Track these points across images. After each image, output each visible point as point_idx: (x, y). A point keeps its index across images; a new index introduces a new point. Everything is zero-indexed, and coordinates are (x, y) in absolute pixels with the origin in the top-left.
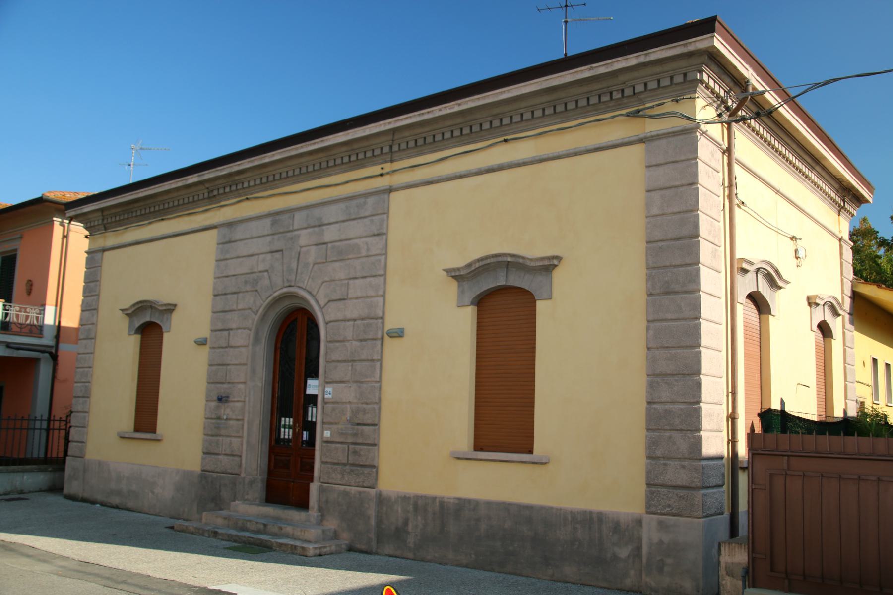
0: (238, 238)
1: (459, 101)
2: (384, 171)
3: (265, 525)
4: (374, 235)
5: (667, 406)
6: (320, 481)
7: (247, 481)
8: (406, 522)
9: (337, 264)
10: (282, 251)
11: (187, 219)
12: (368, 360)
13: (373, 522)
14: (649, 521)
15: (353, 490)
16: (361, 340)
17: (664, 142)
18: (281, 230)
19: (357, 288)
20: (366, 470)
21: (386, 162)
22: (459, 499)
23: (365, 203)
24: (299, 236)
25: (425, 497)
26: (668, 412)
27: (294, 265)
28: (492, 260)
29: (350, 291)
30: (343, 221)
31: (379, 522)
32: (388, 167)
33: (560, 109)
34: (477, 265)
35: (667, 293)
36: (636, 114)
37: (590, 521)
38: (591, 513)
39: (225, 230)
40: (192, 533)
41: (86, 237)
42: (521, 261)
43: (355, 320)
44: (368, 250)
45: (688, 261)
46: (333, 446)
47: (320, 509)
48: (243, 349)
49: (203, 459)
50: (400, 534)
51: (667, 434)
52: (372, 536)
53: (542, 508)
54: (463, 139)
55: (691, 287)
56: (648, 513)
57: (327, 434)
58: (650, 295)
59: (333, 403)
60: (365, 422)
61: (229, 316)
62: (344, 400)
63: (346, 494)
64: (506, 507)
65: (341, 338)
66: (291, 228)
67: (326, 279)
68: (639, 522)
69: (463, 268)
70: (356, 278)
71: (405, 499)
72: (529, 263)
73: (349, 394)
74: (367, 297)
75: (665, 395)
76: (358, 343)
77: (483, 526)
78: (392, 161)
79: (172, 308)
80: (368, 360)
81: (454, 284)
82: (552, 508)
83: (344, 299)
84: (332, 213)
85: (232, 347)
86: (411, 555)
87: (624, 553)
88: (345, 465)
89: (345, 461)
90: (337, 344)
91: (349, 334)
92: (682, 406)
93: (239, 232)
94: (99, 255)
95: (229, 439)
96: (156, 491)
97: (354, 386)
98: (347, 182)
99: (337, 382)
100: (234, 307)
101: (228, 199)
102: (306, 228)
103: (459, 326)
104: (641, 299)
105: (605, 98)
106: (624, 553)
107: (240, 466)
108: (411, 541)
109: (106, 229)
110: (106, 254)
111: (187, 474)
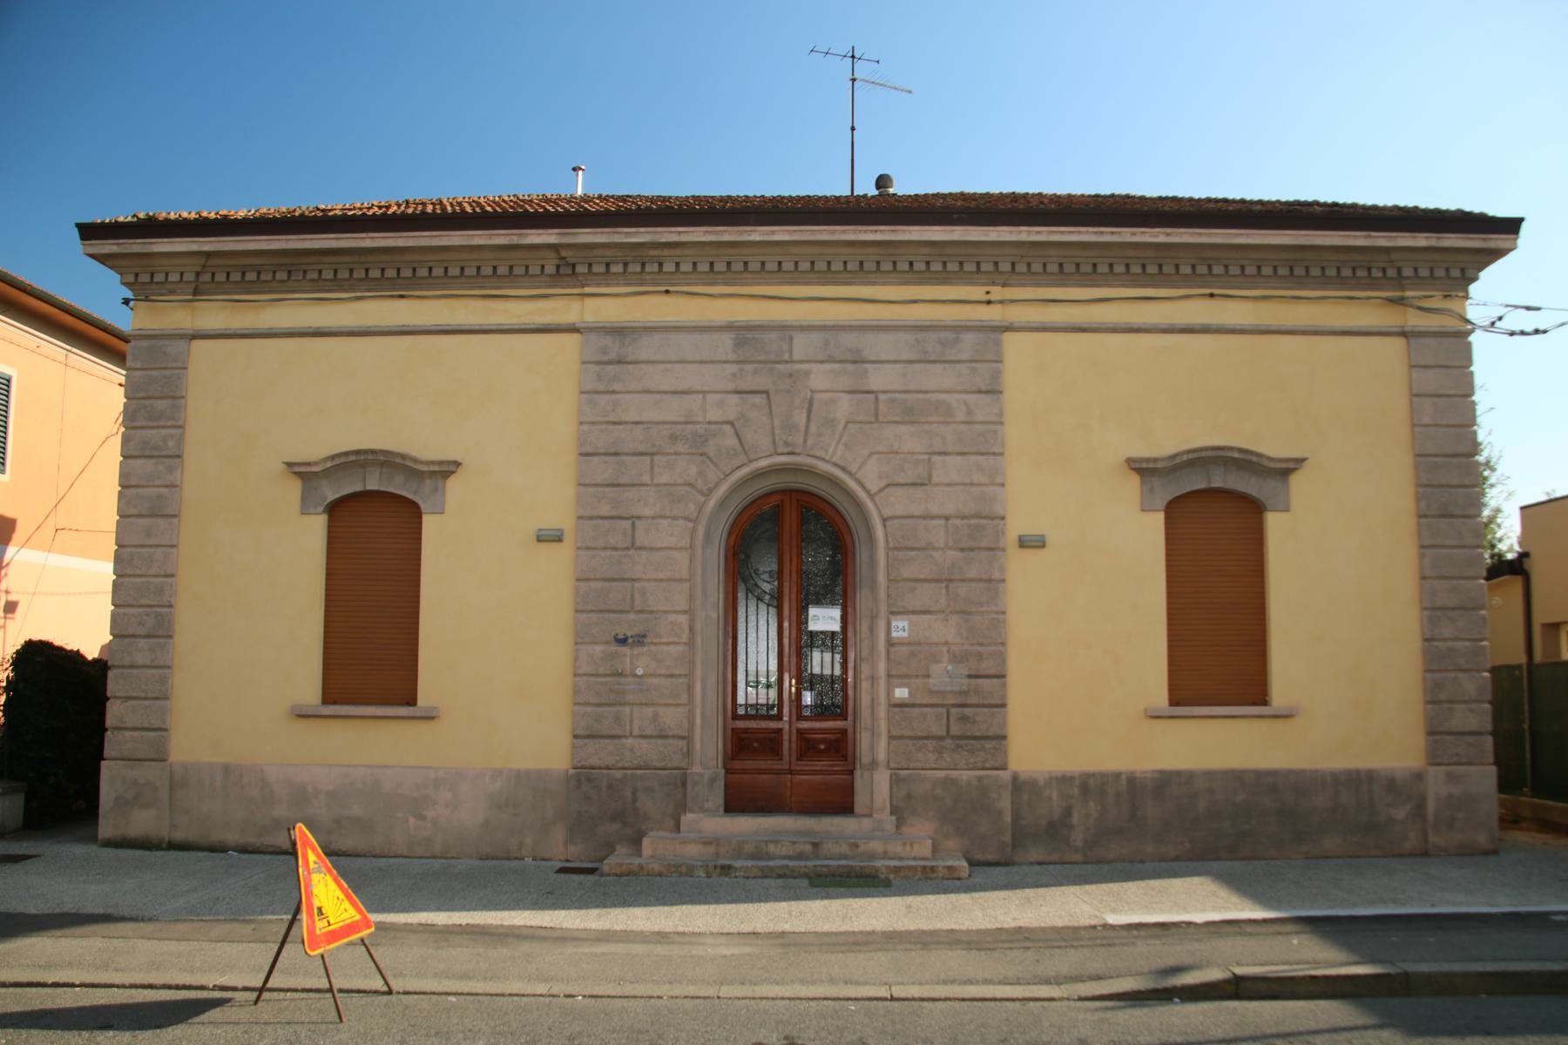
0: (643, 356)
1: (1169, 230)
2: (991, 297)
3: (815, 845)
4: (980, 392)
5: (1450, 644)
6: (888, 767)
7: (706, 778)
8: (1068, 812)
9: (903, 429)
10: (767, 392)
11: (481, 303)
12: (981, 580)
13: (1008, 818)
14: (1435, 775)
15: (965, 775)
16: (962, 550)
17: (1432, 341)
18: (762, 358)
19: (948, 469)
20: (988, 745)
21: (994, 284)
22: (1162, 772)
23: (957, 341)
24: (807, 373)
25: (1102, 775)
26: (1451, 650)
27: (800, 419)
28: (1209, 453)
29: (935, 473)
30: (910, 362)
31: (1017, 816)
32: (997, 293)
33: (1297, 272)
34: (1185, 457)
35: (1443, 516)
36: (1400, 302)
37: (1357, 781)
38: (1358, 772)
39: (607, 341)
40: (660, 875)
41: (126, 302)
42: (1254, 459)
43: (947, 518)
44: (969, 412)
45: (1467, 482)
46: (916, 711)
47: (894, 810)
48: (677, 555)
49: (574, 747)
50: (1056, 830)
51: (1452, 675)
52: (1007, 838)
53: (1290, 772)
54: (1143, 280)
55: (1472, 511)
56: (1432, 764)
57: (901, 693)
58: (1421, 516)
59: (909, 644)
60: (981, 672)
61: (630, 494)
62: (935, 640)
63: (949, 782)
64: (1237, 777)
65: (922, 544)
66: (786, 357)
67: (879, 448)
68: (1419, 776)
69: (1163, 459)
70: (946, 454)
71: (1064, 780)
72: (1265, 463)
73: (945, 631)
74: (972, 484)
75: (1447, 630)
76: (960, 554)
77: (1202, 804)
78: (1004, 285)
79: (452, 468)
80: (981, 580)
81: (1134, 481)
82: (1304, 771)
83: (922, 484)
84: (874, 346)
85: (642, 548)
86: (1078, 857)
87: (1401, 813)
88: (941, 738)
89: (944, 733)
90: (913, 553)
91: (939, 537)
92: (1467, 644)
93: (646, 348)
94: (183, 344)
95: (650, 711)
96: (430, 814)
97: (954, 619)
98: (915, 302)
99: (914, 612)
100: (646, 479)
101: (608, 285)
102: (822, 362)
103: (1143, 538)
104: (1408, 521)
105: (1362, 273)
106: (1401, 813)
107: (689, 753)
108: (1078, 838)
109: (196, 292)
110: (198, 345)
111: (531, 780)
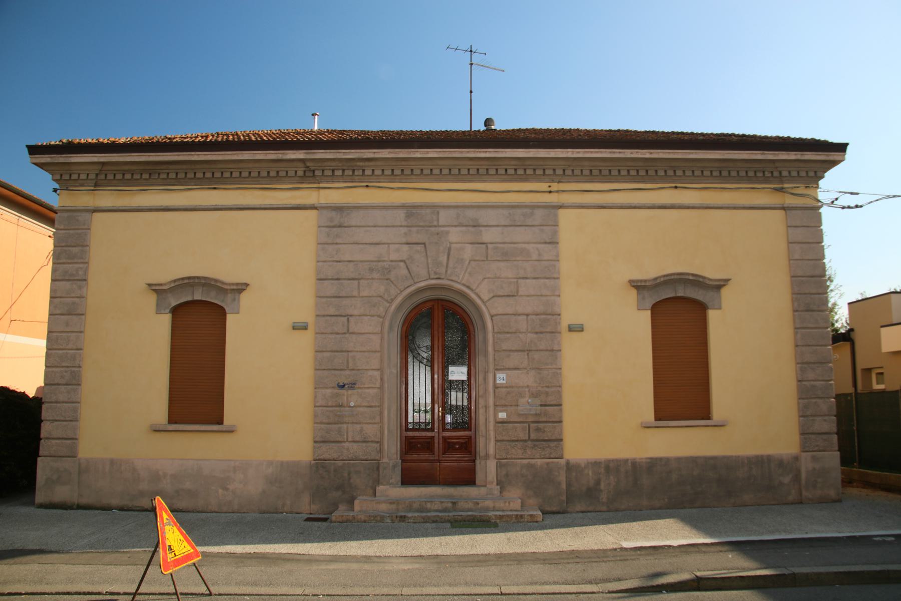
0: (354, 223)
1: (652, 151)
3: (454, 503)
4: (545, 243)
5: (812, 383)
8: (598, 482)
9: (502, 264)
10: (424, 244)
12: (547, 350)
13: (564, 486)
15: (539, 462)
16: (536, 333)
17: (799, 212)
19: (526, 287)
20: (552, 444)
21: (553, 181)
22: (651, 458)
23: (532, 214)
24: (448, 233)
25: (617, 461)
26: (813, 386)
27: (443, 259)
28: (676, 277)
31: (569, 485)
32: (555, 186)
33: (724, 174)
34: (662, 279)
35: (807, 311)
36: (781, 190)
37: (761, 461)
38: (762, 456)
39: (334, 214)
40: (365, 522)
41: (55, 190)
42: (701, 280)
43: (527, 315)
44: (540, 255)
45: (820, 291)
46: (511, 425)
47: (499, 483)
50: (591, 493)
51: (814, 400)
52: (564, 498)
53: (724, 457)
54: (637, 179)
57: (502, 415)
58: (795, 311)
59: (506, 387)
60: (548, 403)
61: (345, 302)
62: (521, 384)
63: (532, 466)
64: (694, 461)
65: (513, 330)
66: (435, 223)
67: (488, 276)
68: (796, 458)
69: (649, 281)
70: (527, 278)
71: (596, 464)
72: (708, 282)
73: (528, 379)
74: (541, 295)
75: (810, 375)
78: (559, 182)
79: (244, 287)
80: (547, 350)
81: (634, 292)
82: (731, 457)
84: (486, 217)
85: (353, 333)
86: (604, 508)
87: (786, 480)
88: (525, 441)
90: (508, 335)
93: (355, 218)
94: (87, 215)
95: (358, 427)
96: (231, 487)
97: (532, 373)
99: (509, 369)
100: (355, 293)
101: (333, 182)
102: (455, 226)
103: (638, 325)
106: (786, 480)
107: (381, 451)
108: (604, 497)
109: (96, 185)
110: (96, 215)
